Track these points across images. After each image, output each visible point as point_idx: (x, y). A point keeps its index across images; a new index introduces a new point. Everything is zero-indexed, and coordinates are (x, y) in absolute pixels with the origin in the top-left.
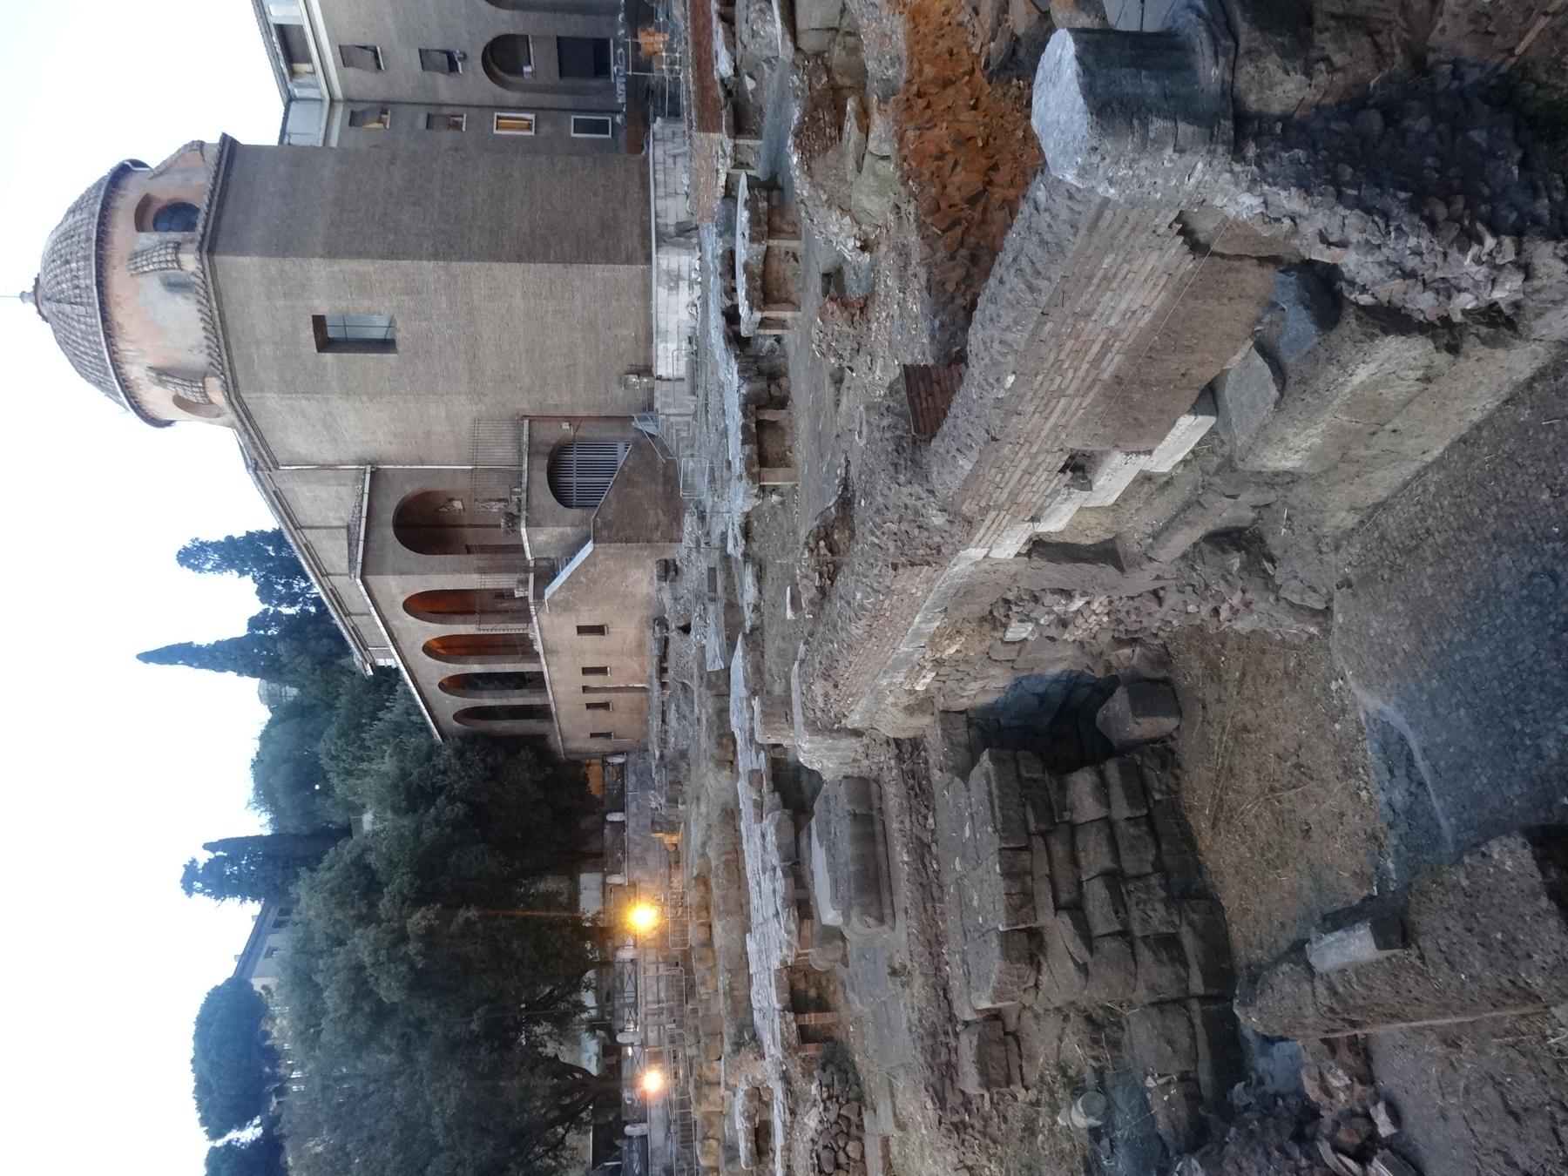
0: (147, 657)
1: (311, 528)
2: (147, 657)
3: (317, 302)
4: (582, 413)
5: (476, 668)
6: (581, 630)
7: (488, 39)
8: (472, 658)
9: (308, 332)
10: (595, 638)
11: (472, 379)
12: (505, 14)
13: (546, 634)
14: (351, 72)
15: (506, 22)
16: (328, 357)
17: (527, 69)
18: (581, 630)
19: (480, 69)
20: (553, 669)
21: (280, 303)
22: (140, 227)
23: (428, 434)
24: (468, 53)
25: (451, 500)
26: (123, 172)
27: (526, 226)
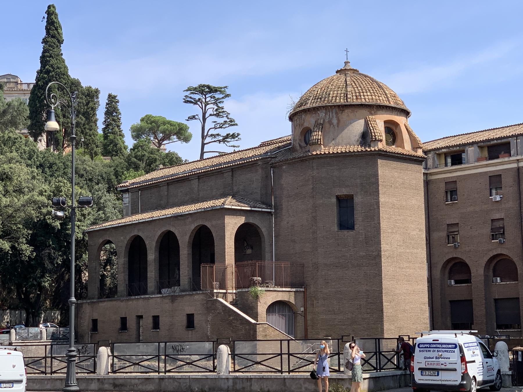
0: (51, 13)
1: (232, 176)
2: (51, 13)
3: (360, 197)
4: (309, 317)
5: (152, 256)
6: (190, 318)
7: (467, 261)
8: (158, 254)
9: (344, 192)
10: (185, 322)
11: (325, 264)
12: (481, 271)
13: (188, 297)
14: (443, 186)
15: (478, 271)
16: (334, 200)
17: (453, 282)
18: (190, 318)
19: (450, 256)
20: (159, 300)
21: (358, 181)
22: (386, 122)
23: (294, 241)
24: (459, 250)
25: (252, 248)
26: (406, 113)
27: (397, 292)
